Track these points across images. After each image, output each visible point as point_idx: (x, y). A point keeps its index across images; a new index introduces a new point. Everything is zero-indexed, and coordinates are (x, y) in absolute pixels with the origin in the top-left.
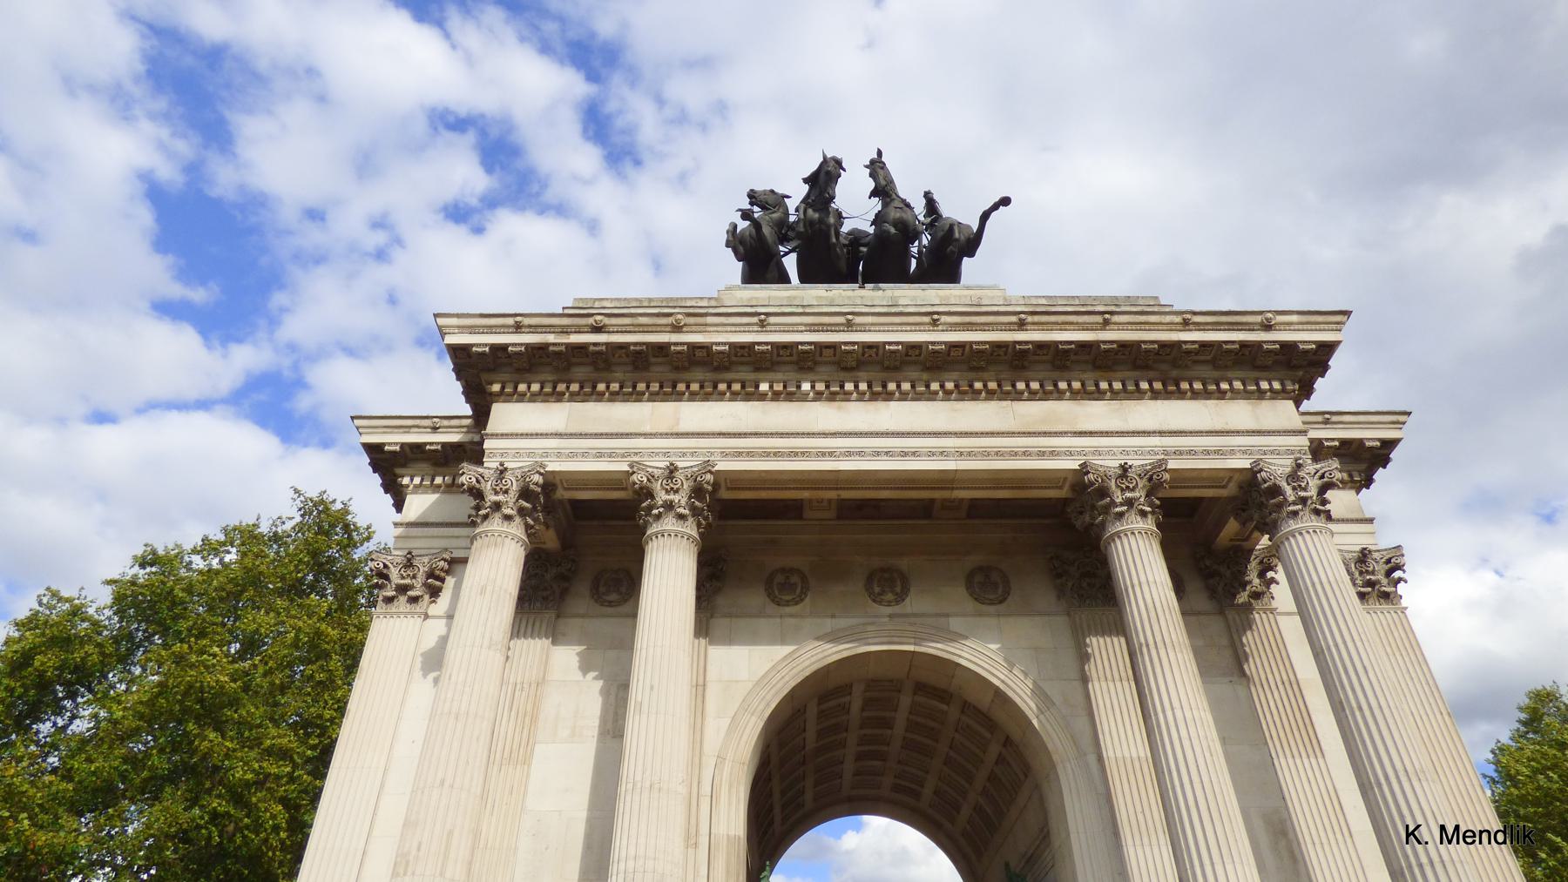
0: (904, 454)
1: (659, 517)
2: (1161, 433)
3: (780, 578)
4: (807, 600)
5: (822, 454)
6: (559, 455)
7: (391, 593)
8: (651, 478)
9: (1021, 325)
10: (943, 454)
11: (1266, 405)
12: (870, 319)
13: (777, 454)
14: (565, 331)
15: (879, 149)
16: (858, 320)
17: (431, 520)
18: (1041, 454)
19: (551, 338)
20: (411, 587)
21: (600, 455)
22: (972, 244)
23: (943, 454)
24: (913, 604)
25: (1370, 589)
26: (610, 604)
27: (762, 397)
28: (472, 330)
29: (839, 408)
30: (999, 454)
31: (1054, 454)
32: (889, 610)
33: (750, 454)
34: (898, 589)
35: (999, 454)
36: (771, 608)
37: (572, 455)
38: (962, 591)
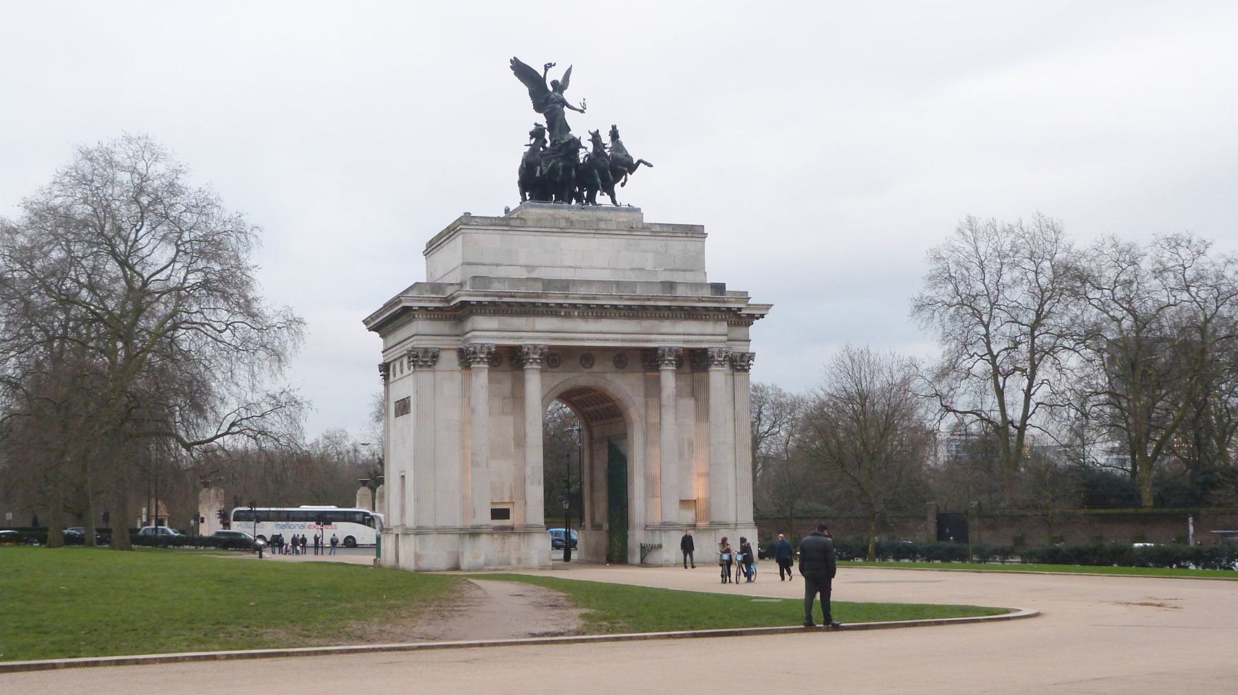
0: (606, 340)
1: (531, 363)
2: (684, 334)
3: (551, 358)
4: (561, 367)
5: (582, 340)
6: (497, 338)
7: (421, 363)
8: (529, 349)
9: (649, 300)
10: (616, 340)
11: (719, 322)
12: (600, 296)
13: (565, 339)
14: (501, 297)
15: (598, 131)
16: (598, 296)
17: (428, 333)
18: (647, 341)
19: (496, 299)
20: (427, 361)
21: (510, 338)
22: (632, 167)
23: (616, 340)
24: (596, 368)
25: (740, 368)
26: (495, 366)
27: (562, 316)
28: (470, 295)
29: (586, 321)
30: (634, 341)
31: (650, 341)
32: (587, 370)
33: (557, 339)
34: (591, 362)
35: (634, 341)
36: (549, 369)
37: (502, 338)
38: (611, 364)
